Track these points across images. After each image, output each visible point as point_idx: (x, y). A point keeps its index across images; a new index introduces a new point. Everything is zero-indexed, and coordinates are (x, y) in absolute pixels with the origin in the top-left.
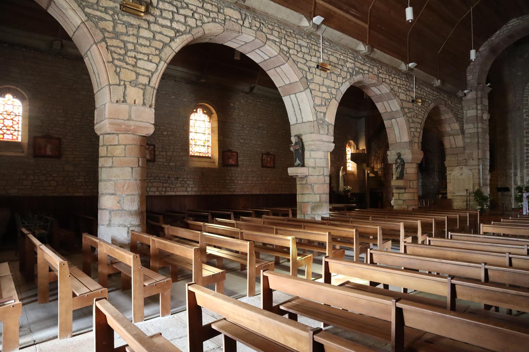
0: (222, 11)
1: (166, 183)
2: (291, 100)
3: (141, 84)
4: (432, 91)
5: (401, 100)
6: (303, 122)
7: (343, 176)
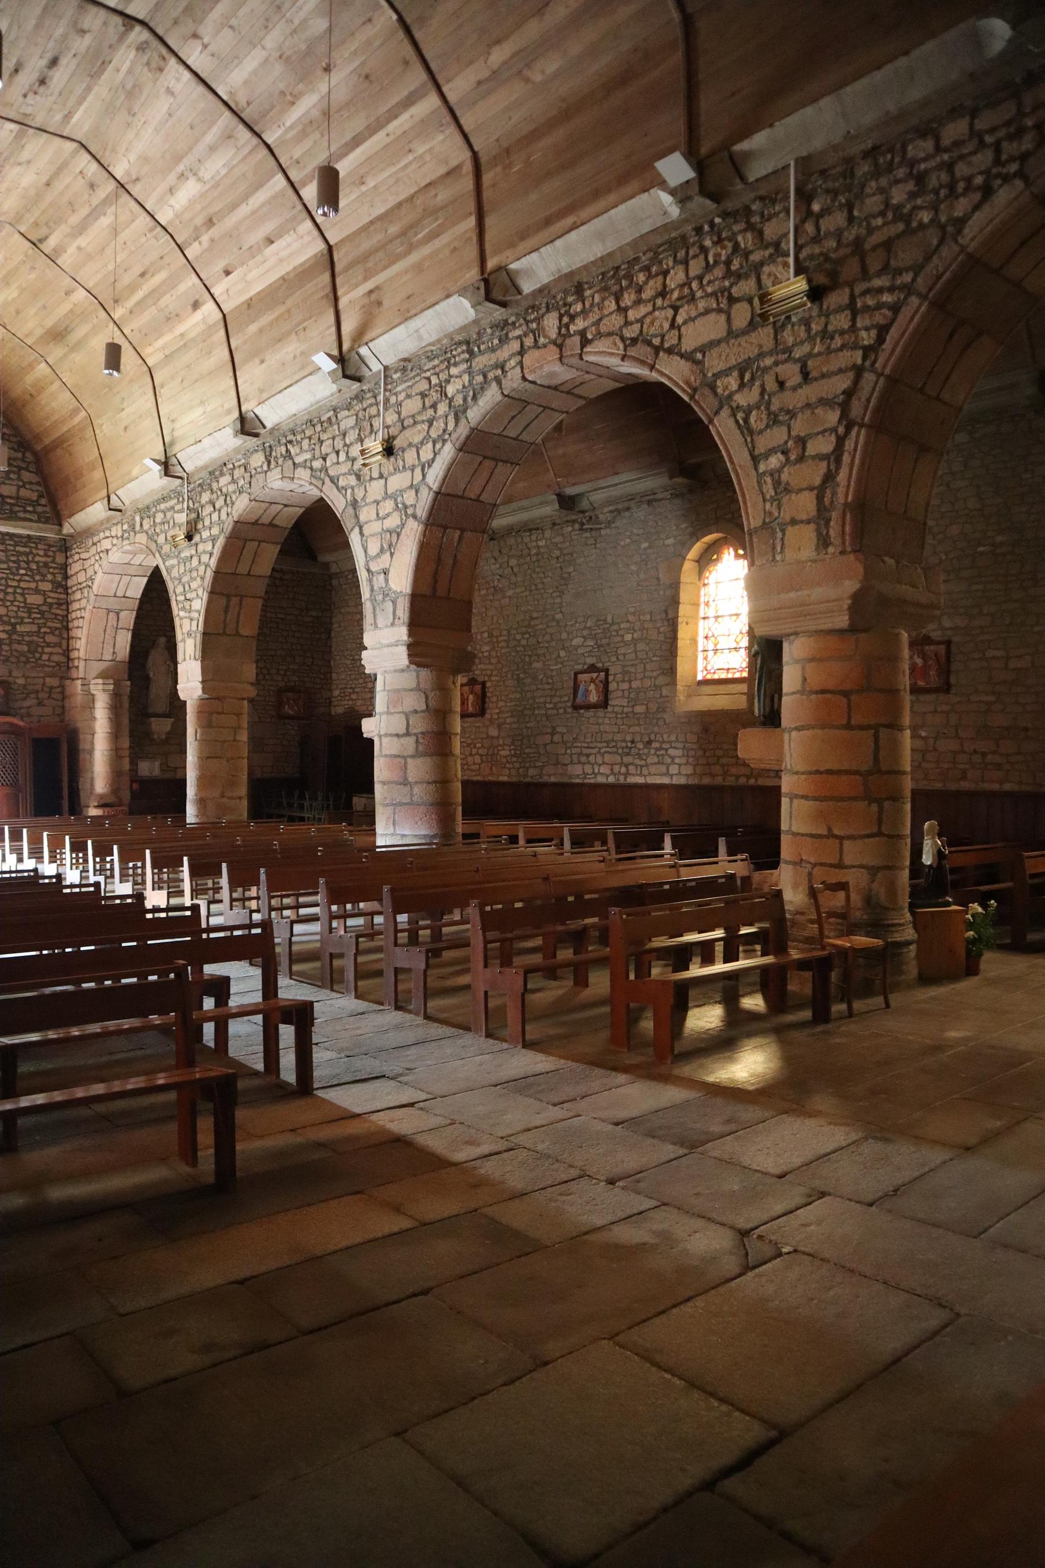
1: (628, 754)
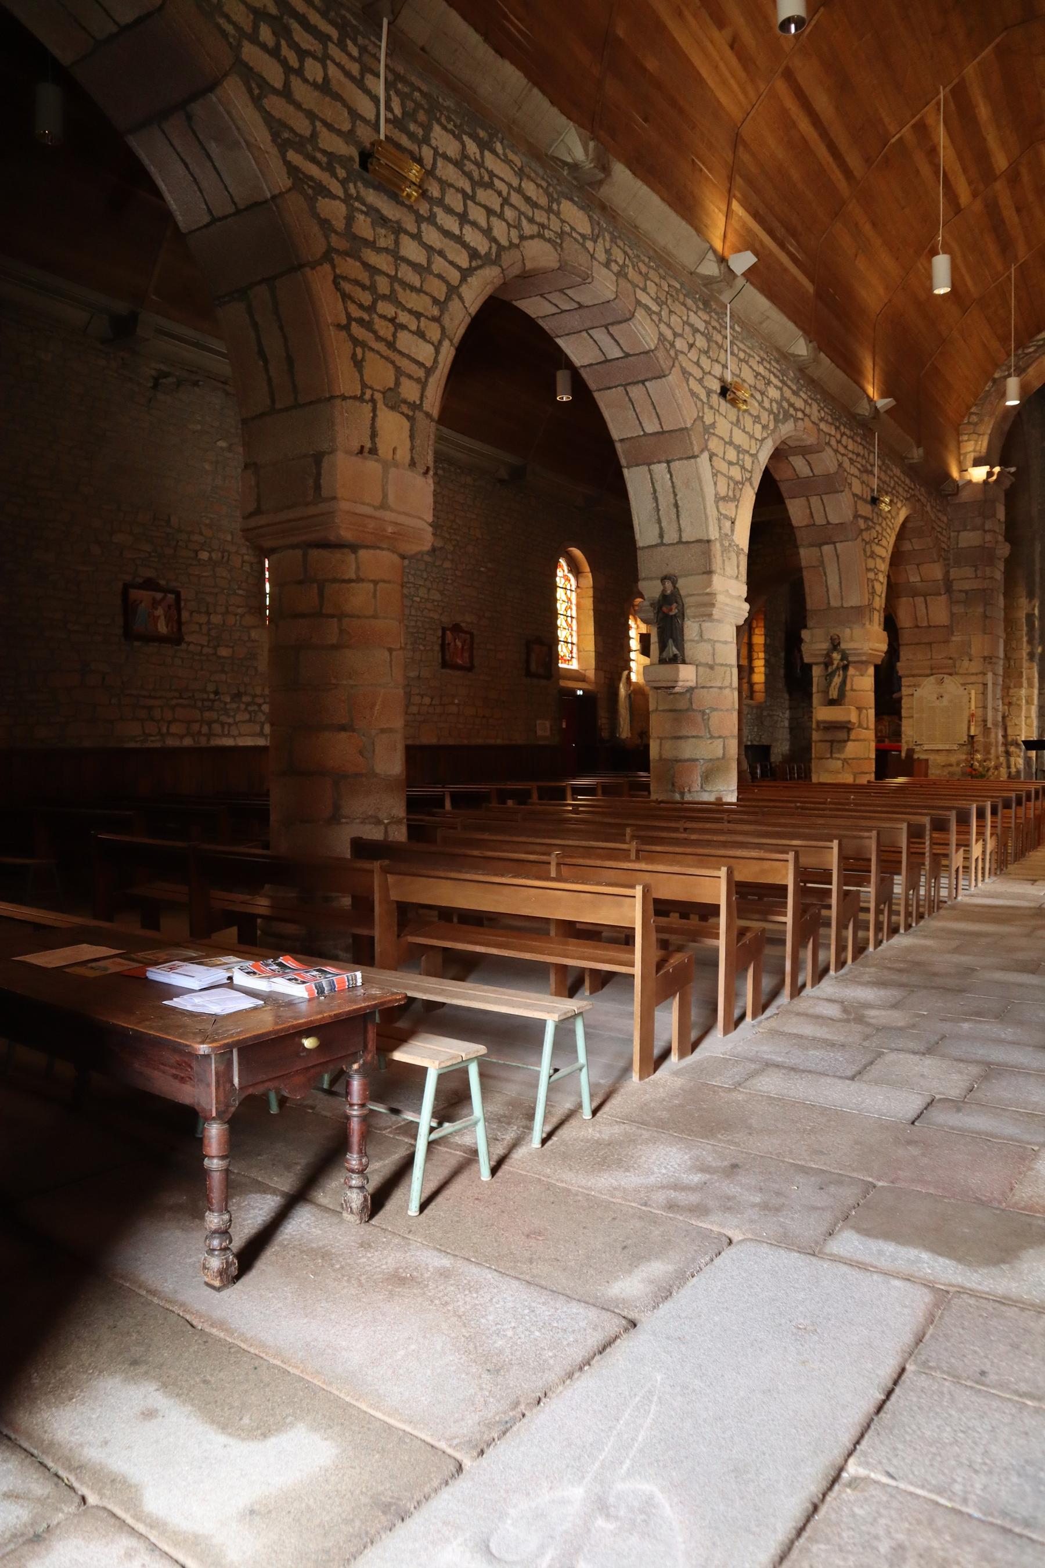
0: (555, 206)
1: (211, 709)
2: (652, 478)
3: (405, 402)
4: (902, 477)
5: (855, 495)
6: (680, 542)
7: (629, 696)
